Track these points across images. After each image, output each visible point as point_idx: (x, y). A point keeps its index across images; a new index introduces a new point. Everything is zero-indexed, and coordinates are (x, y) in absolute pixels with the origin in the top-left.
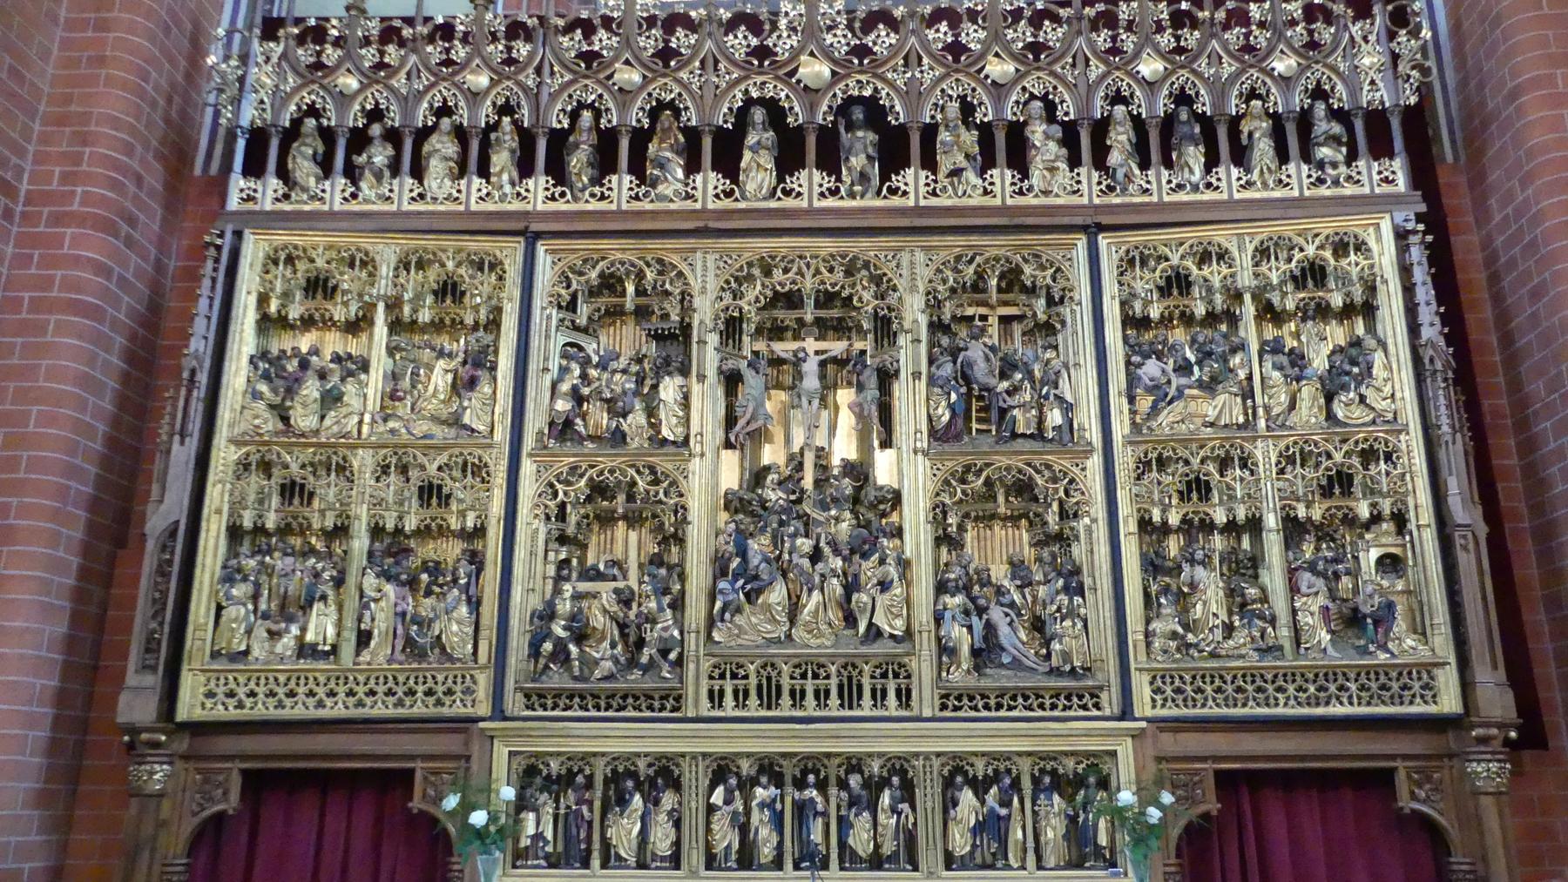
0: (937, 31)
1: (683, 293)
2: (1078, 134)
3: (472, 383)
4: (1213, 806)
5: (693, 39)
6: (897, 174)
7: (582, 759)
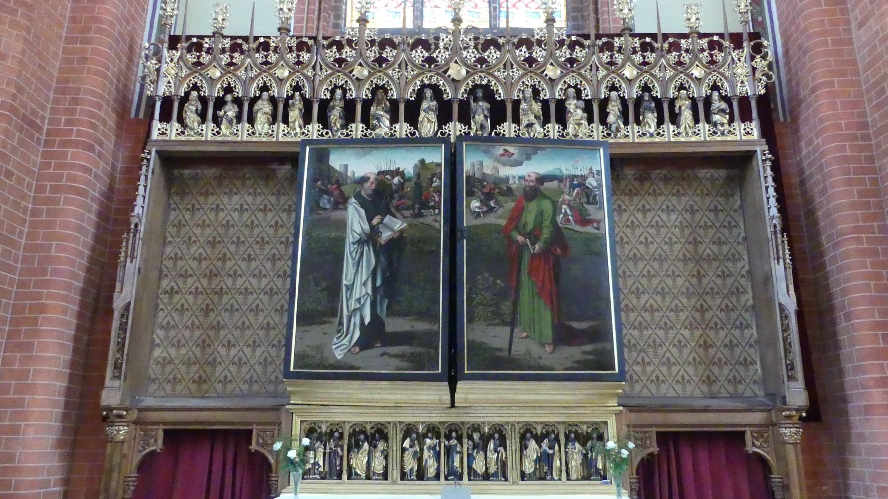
0: (521, 51)
2: (592, 106)
4: (655, 449)
5: (395, 52)
6: (500, 125)
7: (338, 424)
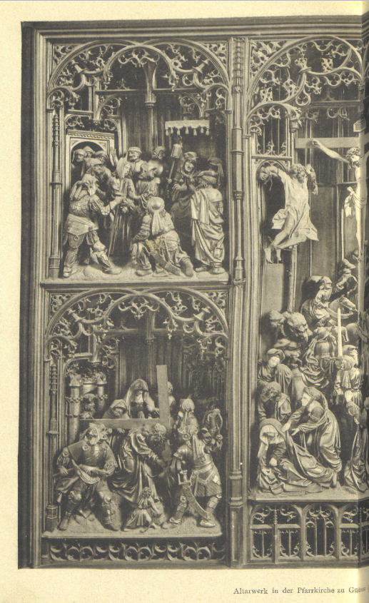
1: (213, 90)
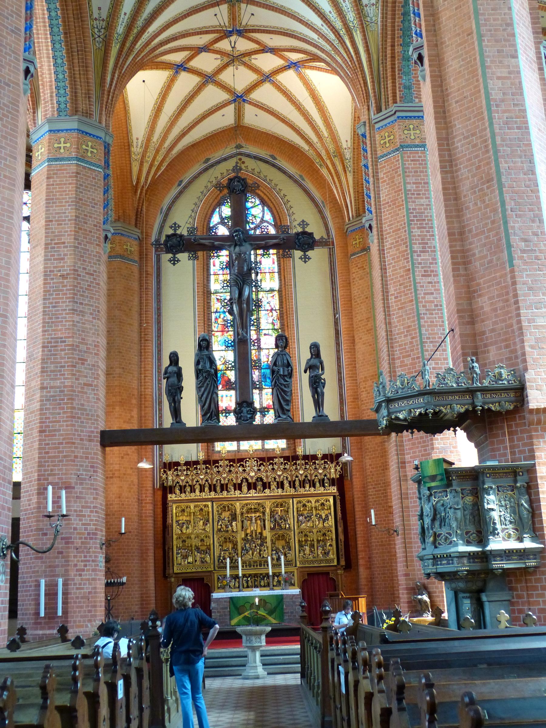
3: (207, 524)
4: (307, 577)
